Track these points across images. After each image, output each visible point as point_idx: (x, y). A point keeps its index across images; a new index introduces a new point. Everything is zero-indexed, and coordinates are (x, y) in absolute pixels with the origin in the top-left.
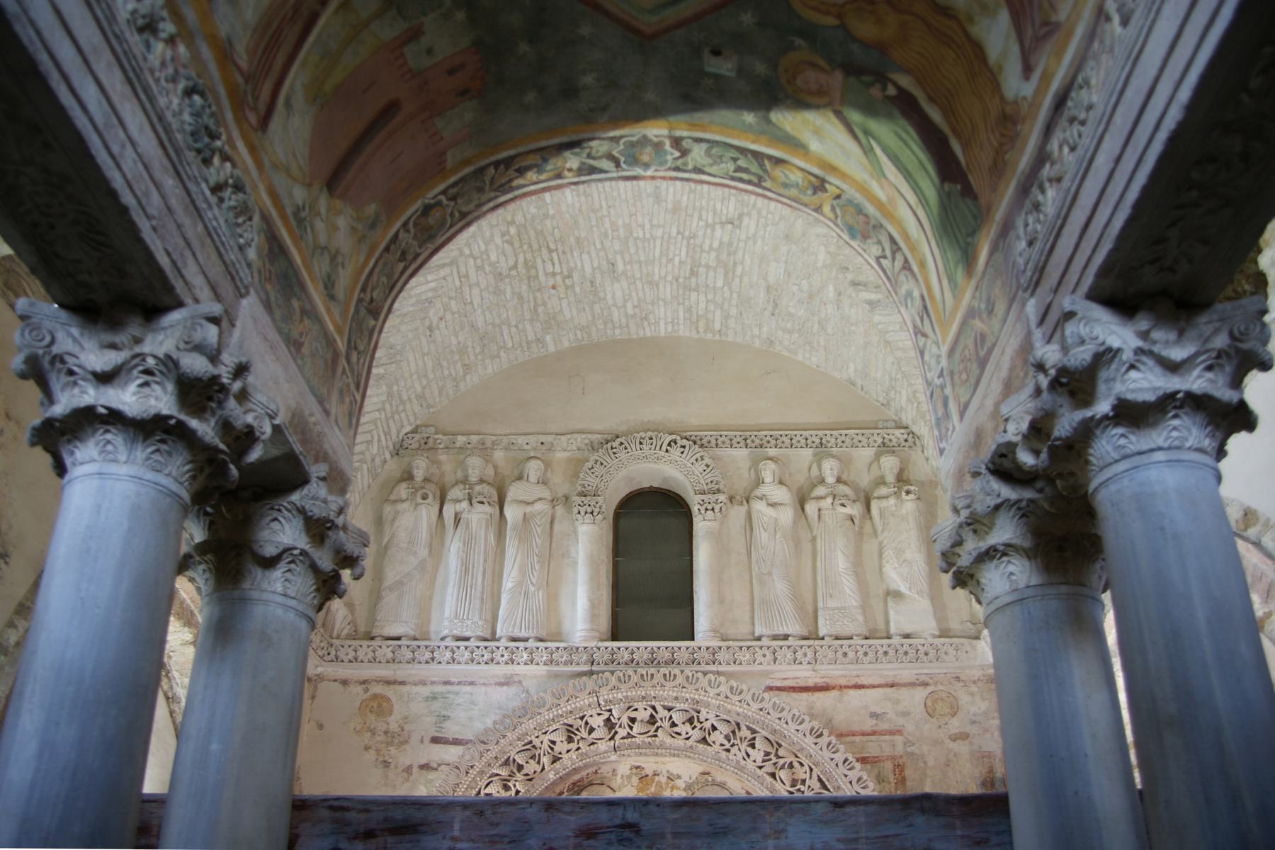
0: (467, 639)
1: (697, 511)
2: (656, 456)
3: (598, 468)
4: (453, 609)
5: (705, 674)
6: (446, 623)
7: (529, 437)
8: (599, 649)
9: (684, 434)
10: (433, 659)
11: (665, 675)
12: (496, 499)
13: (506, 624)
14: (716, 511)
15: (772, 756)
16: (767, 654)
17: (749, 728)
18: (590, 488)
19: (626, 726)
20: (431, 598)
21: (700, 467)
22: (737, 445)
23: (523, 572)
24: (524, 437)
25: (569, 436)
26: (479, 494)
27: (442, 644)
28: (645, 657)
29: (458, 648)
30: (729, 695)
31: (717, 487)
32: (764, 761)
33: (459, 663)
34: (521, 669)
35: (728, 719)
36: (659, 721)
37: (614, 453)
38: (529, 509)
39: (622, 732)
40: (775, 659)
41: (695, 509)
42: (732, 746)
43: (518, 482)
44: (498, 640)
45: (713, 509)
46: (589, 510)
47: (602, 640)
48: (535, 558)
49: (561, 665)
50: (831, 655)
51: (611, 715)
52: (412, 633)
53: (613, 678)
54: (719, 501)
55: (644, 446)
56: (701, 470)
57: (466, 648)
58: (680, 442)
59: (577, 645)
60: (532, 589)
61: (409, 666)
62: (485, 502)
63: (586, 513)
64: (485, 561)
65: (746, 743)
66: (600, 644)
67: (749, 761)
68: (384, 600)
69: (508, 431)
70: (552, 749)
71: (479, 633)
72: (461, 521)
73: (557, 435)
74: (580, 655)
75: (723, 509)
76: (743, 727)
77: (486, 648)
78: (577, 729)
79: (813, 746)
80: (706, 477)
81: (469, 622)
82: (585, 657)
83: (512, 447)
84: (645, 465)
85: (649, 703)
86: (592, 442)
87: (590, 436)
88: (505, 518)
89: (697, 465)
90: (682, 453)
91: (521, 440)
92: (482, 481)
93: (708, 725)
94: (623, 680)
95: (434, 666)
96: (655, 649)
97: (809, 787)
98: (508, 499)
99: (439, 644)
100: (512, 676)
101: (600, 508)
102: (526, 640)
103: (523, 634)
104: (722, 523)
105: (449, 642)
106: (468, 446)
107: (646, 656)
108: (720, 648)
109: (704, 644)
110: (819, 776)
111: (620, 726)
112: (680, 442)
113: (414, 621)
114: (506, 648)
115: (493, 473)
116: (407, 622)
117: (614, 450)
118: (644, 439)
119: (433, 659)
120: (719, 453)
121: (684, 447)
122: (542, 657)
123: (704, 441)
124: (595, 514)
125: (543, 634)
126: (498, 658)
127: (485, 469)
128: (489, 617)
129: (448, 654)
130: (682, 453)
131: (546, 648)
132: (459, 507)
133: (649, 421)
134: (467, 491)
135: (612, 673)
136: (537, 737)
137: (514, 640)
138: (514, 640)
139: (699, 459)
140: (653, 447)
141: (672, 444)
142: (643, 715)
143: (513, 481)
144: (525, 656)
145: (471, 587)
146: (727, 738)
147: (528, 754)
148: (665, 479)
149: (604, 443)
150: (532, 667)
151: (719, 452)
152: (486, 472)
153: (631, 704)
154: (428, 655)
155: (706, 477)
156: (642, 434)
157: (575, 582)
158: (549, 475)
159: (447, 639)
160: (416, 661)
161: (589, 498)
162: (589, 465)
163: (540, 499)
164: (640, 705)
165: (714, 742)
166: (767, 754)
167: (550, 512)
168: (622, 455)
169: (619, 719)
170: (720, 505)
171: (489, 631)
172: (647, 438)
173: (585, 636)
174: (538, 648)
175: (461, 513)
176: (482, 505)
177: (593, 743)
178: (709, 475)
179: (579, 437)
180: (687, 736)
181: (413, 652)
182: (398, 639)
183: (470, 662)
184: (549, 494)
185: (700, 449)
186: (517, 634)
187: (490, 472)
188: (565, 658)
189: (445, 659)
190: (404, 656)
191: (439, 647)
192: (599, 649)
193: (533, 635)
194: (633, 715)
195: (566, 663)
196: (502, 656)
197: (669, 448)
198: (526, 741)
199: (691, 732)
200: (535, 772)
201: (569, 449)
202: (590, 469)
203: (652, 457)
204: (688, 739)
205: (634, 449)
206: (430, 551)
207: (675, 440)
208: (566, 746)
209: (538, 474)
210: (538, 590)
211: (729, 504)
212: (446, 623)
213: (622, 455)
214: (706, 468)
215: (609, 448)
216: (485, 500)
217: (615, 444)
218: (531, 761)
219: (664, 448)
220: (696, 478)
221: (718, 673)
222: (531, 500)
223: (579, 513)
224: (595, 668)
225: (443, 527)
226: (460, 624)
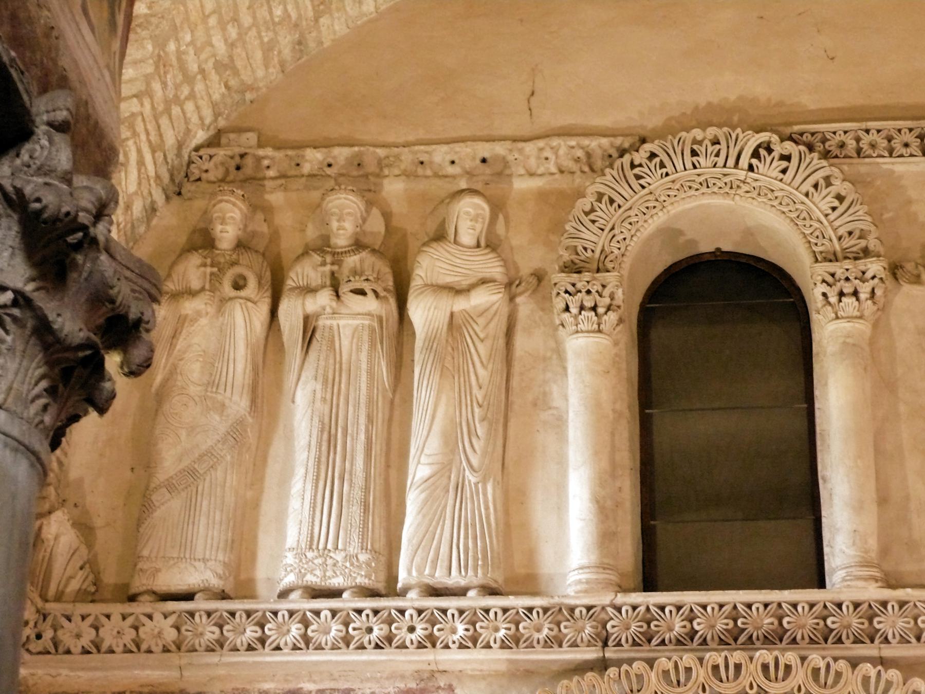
0: (335, 594)
1: (821, 297)
2: (727, 179)
3: (603, 212)
4: (305, 530)
5: (854, 663)
6: (290, 559)
7: (458, 147)
8: (619, 610)
9: (788, 131)
10: (262, 641)
11: (765, 667)
12: (391, 283)
13: (417, 559)
14: (863, 296)
18: (589, 254)
20: (256, 505)
21: (823, 202)
22: (903, 151)
23: (451, 443)
24: (445, 148)
25: (541, 143)
26: (355, 272)
27: (284, 606)
28: (720, 626)
29: (317, 613)
31: (863, 243)
33: (319, 648)
34: (453, 658)
37: (638, 177)
38: (461, 304)
41: (814, 294)
43: (435, 245)
44: (403, 593)
45: (855, 293)
46: (589, 304)
47: (625, 590)
48: (477, 410)
49: (538, 648)
52: (215, 583)
53: (653, 675)
54: (869, 275)
55: (702, 159)
56: (825, 206)
57: (334, 613)
58: (780, 148)
59: (572, 602)
60: (471, 477)
61: (213, 658)
62: (367, 291)
63: (582, 308)
64: (370, 419)
66: (621, 599)
68: (157, 514)
69: (411, 138)
71: (361, 580)
72: (318, 335)
73: (515, 140)
74: (580, 623)
75: (879, 292)
77: (376, 612)
80: (837, 223)
81: (339, 557)
82: (588, 630)
83: (420, 171)
84: (705, 201)
86: (589, 155)
87: (586, 142)
88: (411, 323)
89: (817, 197)
90: (784, 171)
91: (440, 155)
92: (358, 245)
94: (675, 682)
95: (266, 657)
96: (740, 607)
98: (416, 283)
99: (275, 607)
100: (432, 674)
101: (612, 297)
102: (461, 592)
103: (455, 579)
104: (875, 325)
105: (297, 602)
106: (329, 171)
107: (722, 624)
108: (884, 604)
109: (847, 597)
112: (780, 148)
113: (221, 557)
114: (420, 612)
115: (382, 230)
116: (205, 560)
117: (637, 171)
118: (700, 143)
119: (262, 641)
120: (863, 169)
121: (787, 158)
122: (497, 630)
123: (831, 145)
124: (601, 310)
125: (496, 577)
126: (402, 635)
127: (364, 220)
128: (380, 545)
129: (295, 629)
130: (784, 171)
131: (505, 610)
132: (313, 304)
133: (709, 104)
134: (328, 268)
135: (651, 663)
137: (435, 592)
138: (435, 592)
139: (822, 183)
140: (721, 160)
141: (763, 152)
143: (425, 244)
144: (461, 628)
148: (749, 233)
149: (615, 155)
150: (477, 655)
151: (863, 167)
152: (368, 227)
154: (251, 633)
155: (837, 223)
156: (697, 133)
157: (562, 463)
158: (500, 228)
159: (294, 596)
160: (225, 647)
161: (586, 276)
162: (585, 203)
163: (484, 281)
167: (505, 311)
168: (655, 182)
170: (872, 283)
171: (382, 576)
172: (707, 142)
173: (588, 582)
174: (487, 611)
175: (317, 316)
176: (360, 297)
178: (846, 218)
179: (562, 145)
181: (221, 627)
182: (189, 596)
183: (342, 645)
184: (499, 269)
185: (824, 163)
186: (440, 578)
187: (376, 225)
188: (545, 631)
189: (289, 639)
190: (202, 634)
191: (275, 613)
192: (619, 610)
193: (476, 581)
195: (548, 644)
196: (412, 629)
197: (754, 162)
201: (541, 170)
202: (587, 214)
203: (719, 184)
205: (680, 166)
206: (253, 401)
207: (769, 143)
209: (479, 227)
210: (484, 481)
211: (890, 282)
212: (290, 559)
213: (655, 182)
214: (836, 203)
215: (627, 166)
216: (367, 287)
217: (640, 157)
219: (744, 162)
220: (816, 225)
221: (883, 662)
222: (465, 283)
223: (567, 309)
224: (610, 654)
225: (280, 348)
226: (320, 561)
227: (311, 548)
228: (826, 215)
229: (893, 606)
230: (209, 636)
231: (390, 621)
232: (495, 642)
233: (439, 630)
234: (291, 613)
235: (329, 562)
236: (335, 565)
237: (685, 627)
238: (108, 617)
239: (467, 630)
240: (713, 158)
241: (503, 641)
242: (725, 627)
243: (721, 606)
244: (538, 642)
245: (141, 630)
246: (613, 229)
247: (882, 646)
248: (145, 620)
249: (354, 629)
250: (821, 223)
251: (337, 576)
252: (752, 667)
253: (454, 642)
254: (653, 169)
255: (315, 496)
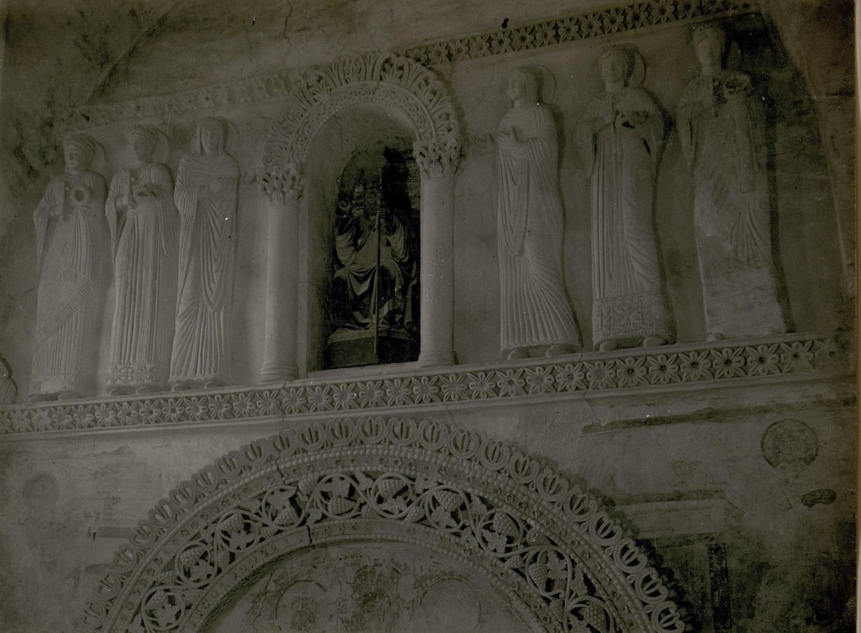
8: (288, 391)
15: (518, 543)
16: (515, 380)
17: (483, 500)
19: (319, 505)
23: (197, 287)
30: (453, 450)
32: (508, 550)
35: (454, 488)
36: (362, 494)
39: (316, 515)
40: (525, 388)
42: (463, 527)
50: (608, 374)
51: (298, 490)
59: (261, 388)
65: (481, 524)
67: (488, 551)
70: (227, 542)
76: (477, 501)
78: (257, 514)
79: (576, 527)
85: (346, 469)
93: (427, 498)
97: (571, 592)
110: (585, 576)
111: (312, 506)
117: (311, 90)
119: (95, 421)
122: (222, 408)
136: (206, 528)
142: (342, 488)
145: (138, 317)
146: (454, 515)
147: (198, 551)
153: (322, 473)
154: (88, 418)
164: (335, 473)
165: (437, 523)
166: (510, 540)
169: (309, 496)
177: (279, 532)
180: (401, 515)
192: (288, 391)
194: (326, 488)
197: (383, 74)
198: (193, 534)
199: (406, 510)
200: (209, 576)
204: (402, 519)
205: (338, 83)
208: (244, 538)
210: (219, 310)
218: (202, 562)
219: (376, 75)
220: (420, 113)
227: (120, 362)
228: (426, 106)
229: (453, 377)
230: (66, 421)
231: (160, 406)
232: (220, 415)
233: (188, 410)
234: (107, 404)
235: (130, 371)
236: (132, 372)
237: (328, 399)
238: (15, 412)
239: (204, 409)
240: (358, 75)
241: (225, 415)
242: (351, 398)
243: (348, 384)
244: (245, 414)
245: (33, 418)
246: (298, 131)
247: (448, 403)
248: (33, 413)
249: (142, 412)
250: (424, 112)
251: (133, 380)
252: (356, 428)
253: (198, 417)
254: (322, 88)
255: (123, 327)
